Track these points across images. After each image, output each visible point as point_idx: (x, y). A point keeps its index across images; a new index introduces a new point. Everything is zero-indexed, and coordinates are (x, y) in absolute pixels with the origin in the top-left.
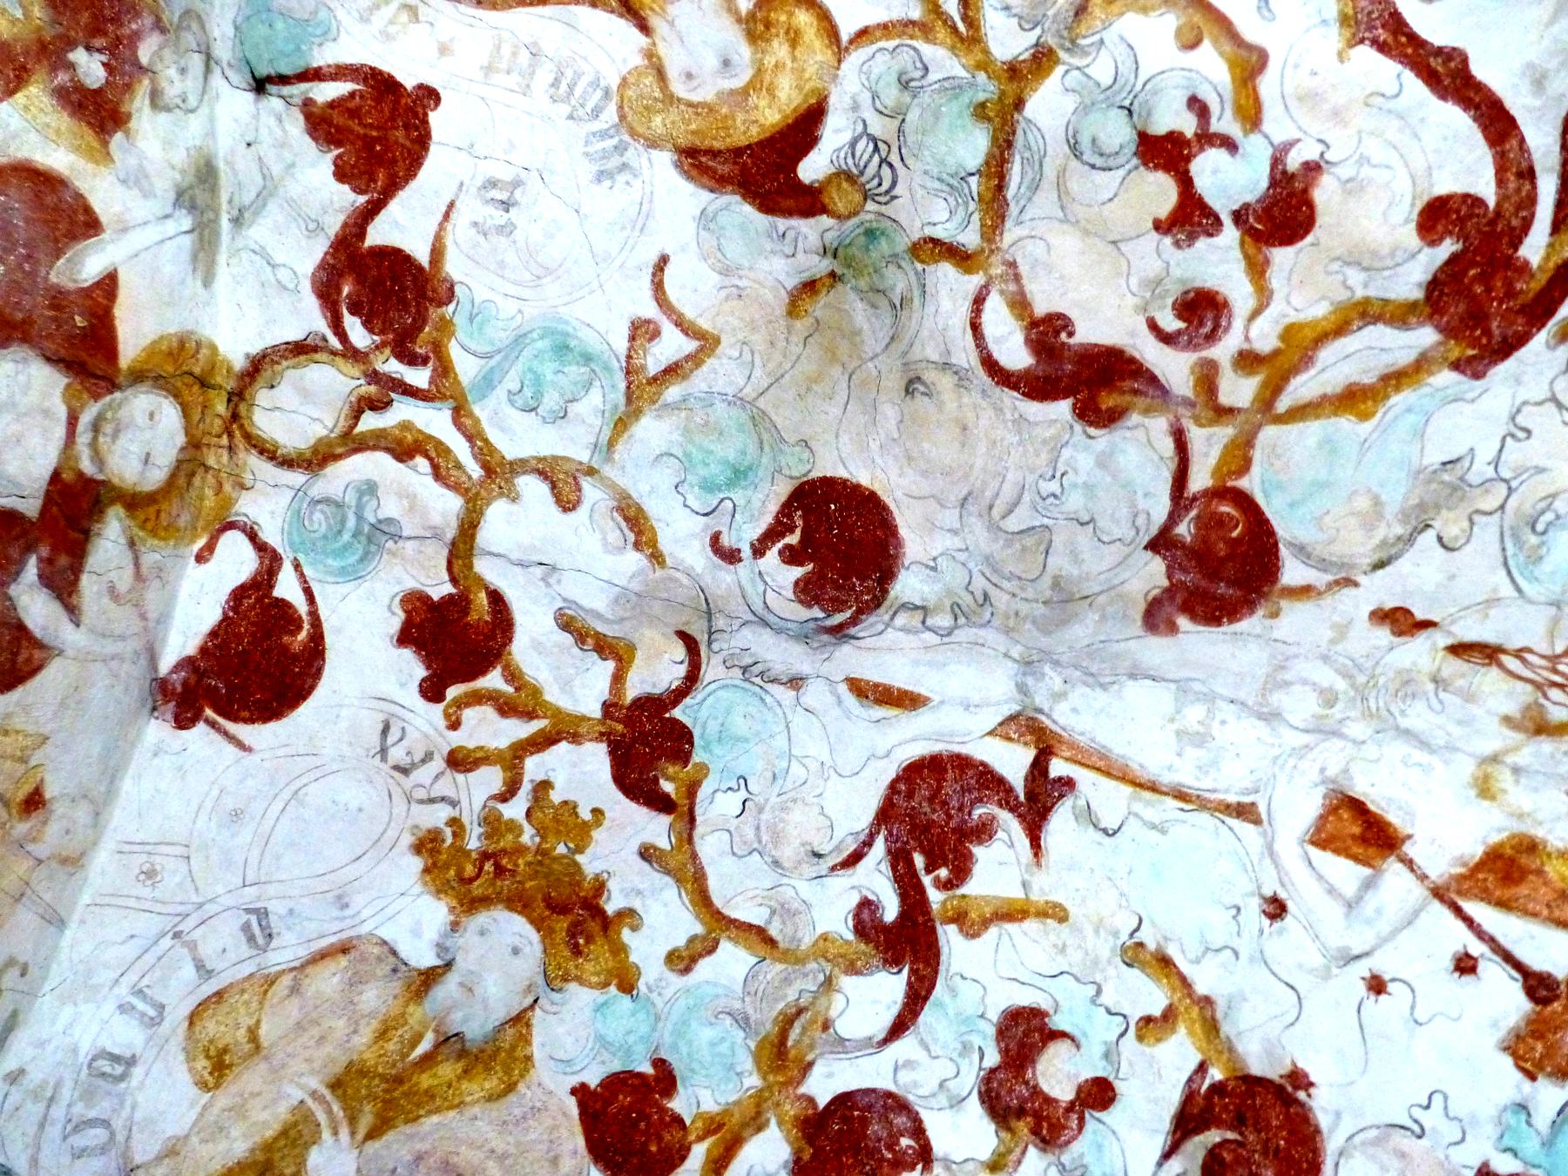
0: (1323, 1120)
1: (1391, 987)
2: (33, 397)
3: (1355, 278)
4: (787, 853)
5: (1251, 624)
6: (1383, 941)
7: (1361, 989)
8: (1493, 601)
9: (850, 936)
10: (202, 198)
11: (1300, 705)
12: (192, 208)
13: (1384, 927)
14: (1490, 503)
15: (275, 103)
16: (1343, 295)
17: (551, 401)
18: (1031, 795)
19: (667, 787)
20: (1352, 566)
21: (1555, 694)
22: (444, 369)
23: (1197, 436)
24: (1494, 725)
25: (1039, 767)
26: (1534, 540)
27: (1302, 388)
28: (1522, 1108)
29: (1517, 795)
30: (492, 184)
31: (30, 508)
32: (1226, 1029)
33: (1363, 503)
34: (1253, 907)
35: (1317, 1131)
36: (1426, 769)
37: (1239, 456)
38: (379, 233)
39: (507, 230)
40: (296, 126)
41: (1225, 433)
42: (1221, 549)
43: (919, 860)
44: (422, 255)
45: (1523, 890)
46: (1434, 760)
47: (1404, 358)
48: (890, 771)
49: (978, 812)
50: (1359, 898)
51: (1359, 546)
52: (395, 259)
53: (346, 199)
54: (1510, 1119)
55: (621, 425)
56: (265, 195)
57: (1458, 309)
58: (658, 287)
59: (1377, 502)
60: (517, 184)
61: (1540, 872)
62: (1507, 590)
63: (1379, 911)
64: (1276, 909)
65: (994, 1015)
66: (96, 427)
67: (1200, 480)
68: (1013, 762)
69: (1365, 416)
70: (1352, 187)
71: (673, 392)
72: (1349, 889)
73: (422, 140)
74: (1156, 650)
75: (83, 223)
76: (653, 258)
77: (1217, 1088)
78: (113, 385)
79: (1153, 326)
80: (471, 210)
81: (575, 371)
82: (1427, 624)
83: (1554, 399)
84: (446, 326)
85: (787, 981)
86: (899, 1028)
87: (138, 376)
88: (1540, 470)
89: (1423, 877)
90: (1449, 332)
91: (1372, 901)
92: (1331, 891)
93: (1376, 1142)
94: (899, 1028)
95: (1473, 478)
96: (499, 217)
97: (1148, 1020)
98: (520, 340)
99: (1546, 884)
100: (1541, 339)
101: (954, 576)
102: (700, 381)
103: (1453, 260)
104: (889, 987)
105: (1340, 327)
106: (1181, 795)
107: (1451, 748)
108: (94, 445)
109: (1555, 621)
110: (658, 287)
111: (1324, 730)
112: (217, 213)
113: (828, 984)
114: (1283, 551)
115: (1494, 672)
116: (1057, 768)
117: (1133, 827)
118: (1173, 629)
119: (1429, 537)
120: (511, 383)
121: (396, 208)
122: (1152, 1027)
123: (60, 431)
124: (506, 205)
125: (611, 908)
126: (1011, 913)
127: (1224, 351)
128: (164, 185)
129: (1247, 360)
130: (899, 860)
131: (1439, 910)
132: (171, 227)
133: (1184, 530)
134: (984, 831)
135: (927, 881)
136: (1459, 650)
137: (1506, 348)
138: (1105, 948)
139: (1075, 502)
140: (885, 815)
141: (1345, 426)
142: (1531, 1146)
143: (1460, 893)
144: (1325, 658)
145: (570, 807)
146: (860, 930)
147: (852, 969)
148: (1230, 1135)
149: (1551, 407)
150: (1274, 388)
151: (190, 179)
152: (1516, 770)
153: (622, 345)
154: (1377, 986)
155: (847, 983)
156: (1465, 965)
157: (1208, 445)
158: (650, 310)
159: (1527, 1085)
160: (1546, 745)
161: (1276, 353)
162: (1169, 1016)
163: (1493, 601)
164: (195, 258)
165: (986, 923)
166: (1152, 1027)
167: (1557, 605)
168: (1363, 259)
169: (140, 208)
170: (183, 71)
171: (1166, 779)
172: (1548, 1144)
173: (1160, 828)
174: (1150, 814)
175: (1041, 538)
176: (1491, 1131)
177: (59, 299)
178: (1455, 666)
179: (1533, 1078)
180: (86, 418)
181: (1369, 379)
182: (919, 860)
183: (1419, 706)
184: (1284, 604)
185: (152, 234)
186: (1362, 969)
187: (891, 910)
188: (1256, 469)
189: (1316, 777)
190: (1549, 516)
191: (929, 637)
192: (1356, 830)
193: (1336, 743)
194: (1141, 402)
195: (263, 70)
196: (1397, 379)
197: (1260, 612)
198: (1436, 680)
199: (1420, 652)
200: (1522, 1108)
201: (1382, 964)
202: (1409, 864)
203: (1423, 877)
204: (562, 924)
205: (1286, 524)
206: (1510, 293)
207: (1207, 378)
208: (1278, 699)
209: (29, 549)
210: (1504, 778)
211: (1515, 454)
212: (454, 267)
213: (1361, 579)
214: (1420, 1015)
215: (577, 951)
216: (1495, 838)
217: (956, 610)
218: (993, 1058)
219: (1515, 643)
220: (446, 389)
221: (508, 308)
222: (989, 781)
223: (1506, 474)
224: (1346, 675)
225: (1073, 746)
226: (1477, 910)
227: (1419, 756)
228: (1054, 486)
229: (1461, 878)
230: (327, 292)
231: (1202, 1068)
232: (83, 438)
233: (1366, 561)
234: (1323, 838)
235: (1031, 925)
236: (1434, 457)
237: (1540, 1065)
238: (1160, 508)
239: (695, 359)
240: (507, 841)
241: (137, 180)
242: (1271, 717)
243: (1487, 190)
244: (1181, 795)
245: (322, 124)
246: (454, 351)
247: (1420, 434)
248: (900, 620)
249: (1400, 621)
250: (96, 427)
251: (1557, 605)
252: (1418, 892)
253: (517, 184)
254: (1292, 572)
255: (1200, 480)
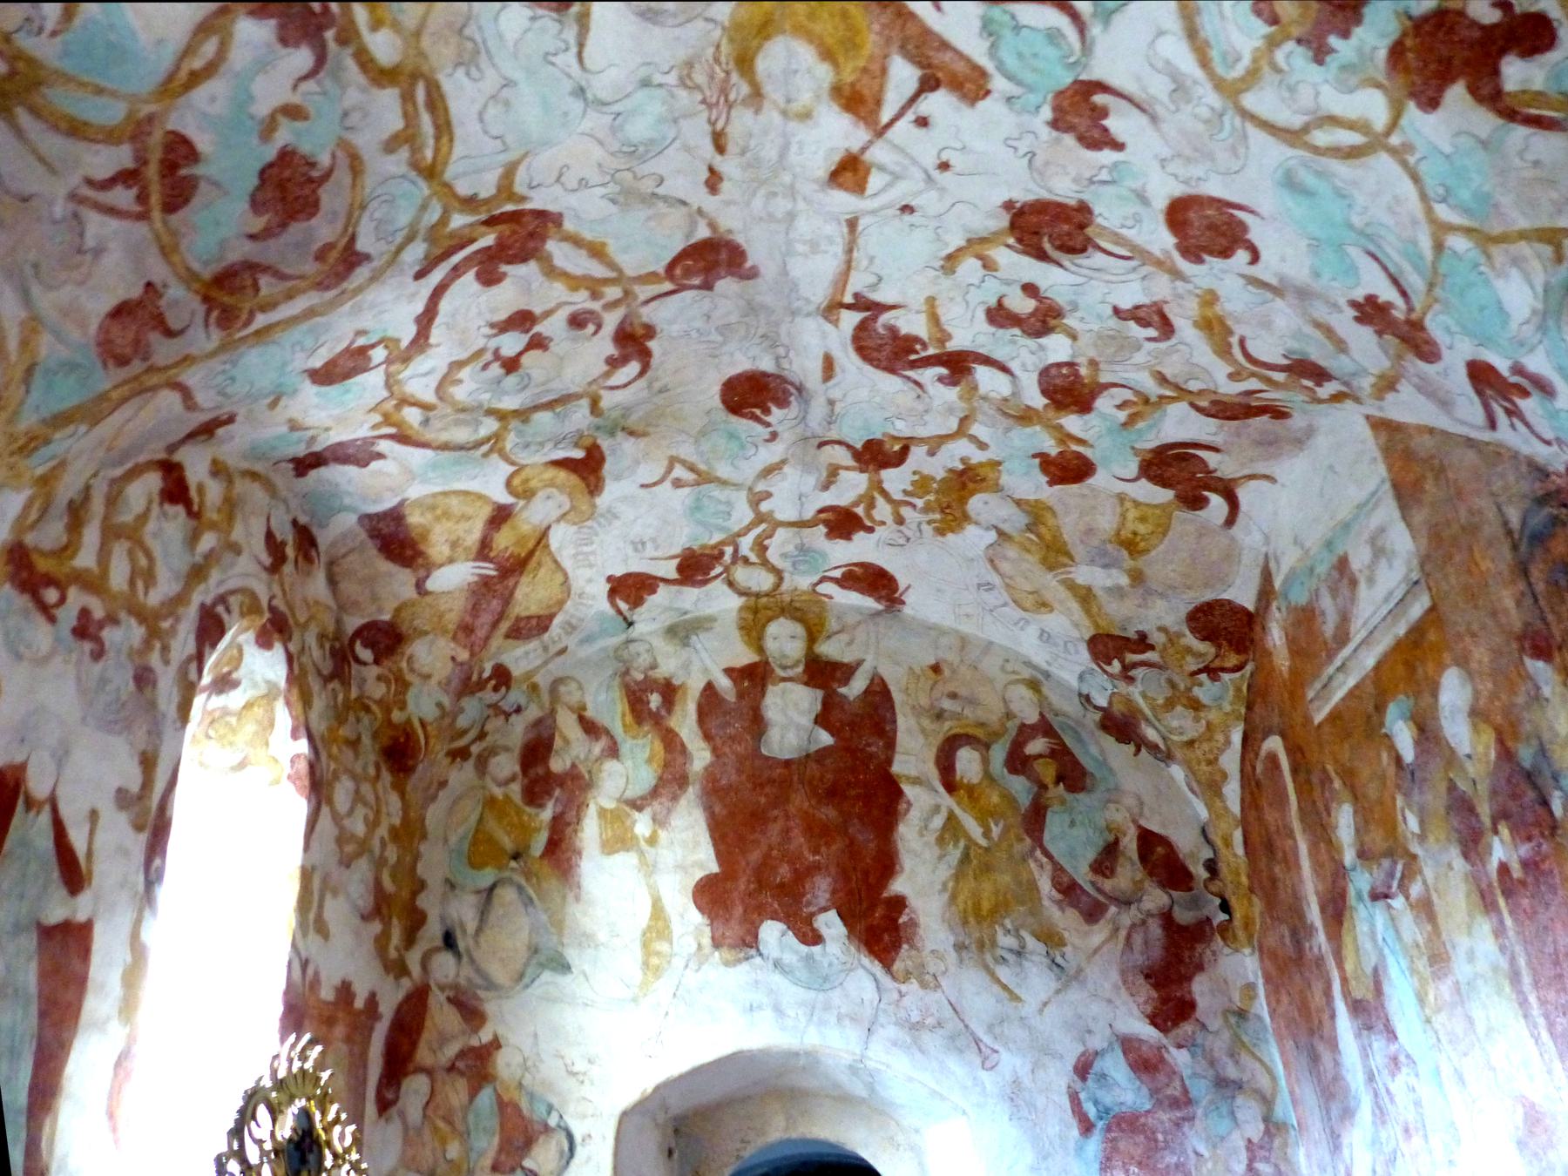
0: (1030, 197)
1: (944, 157)
2: (778, 701)
3: (535, 286)
4: (921, 408)
5: (740, 239)
6: (914, 162)
7: (947, 174)
8: (687, 149)
9: (958, 389)
10: (682, 634)
11: (781, 205)
12: (687, 637)
13: (906, 162)
14: (628, 175)
15: (635, 618)
16: (547, 284)
17: (722, 508)
18: (867, 309)
19: (897, 448)
20: (690, 216)
21: (732, 97)
22: (723, 543)
23: (642, 297)
24: (762, 118)
25: (849, 307)
26: (641, 149)
27: (598, 270)
28: (1009, 100)
29: (805, 98)
30: (636, 550)
31: (819, 694)
32: (985, 235)
33: (652, 224)
34: (907, 218)
35: (1037, 201)
36: (801, 144)
37: (651, 277)
38: (674, 575)
39: (653, 540)
40: (639, 610)
41: (637, 288)
42: (701, 264)
43: (913, 357)
44: (677, 561)
45: (866, 92)
46: (794, 140)
47: (566, 247)
48: (868, 369)
49: (881, 331)
50: (892, 173)
51: (677, 215)
52: (680, 569)
53: (663, 590)
54: (1017, 107)
55: (724, 483)
56: (670, 609)
57: (531, 245)
58: (655, 484)
59: (649, 218)
60: (633, 543)
61: (853, 85)
62: (677, 144)
63: (897, 163)
64: (907, 209)
65: (993, 329)
66: (784, 668)
67: (668, 286)
68: (850, 319)
69: (604, 245)
70: (493, 311)
71: (702, 467)
72: (887, 178)
73: (629, 575)
74: (769, 270)
75: (709, 688)
76: (643, 492)
77: (1020, 240)
78: (767, 663)
79: (596, 333)
80: (650, 551)
81: (706, 501)
82: (711, 170)
83: (558, 180)
84: (703, 547)
85: (985, 414)
86: (1004, 369)
87: (761, 650)
88: (600, 165)
89: (871, 142)
90: (543, 239)
91: (892, 167)
92: (889, 185)
93: (1041, 174)
94: (1004, 369)
95: (617, 188)
96: (649, 545)
97: (985, 267)
98: (700, 523)
99: (859, 80)
100: (528, 206)
101: (755, 351)
102: (693, 458)
103: (509, 263)
104: (982, 374)
105: (564, 275)
106: (850, 251)
107: (784, 135)
108: (792, 667)
109: (685, 116)
110: (655, 484)
111: (792, 192)
112: (686, 621)
113: (985, 398)
114: (693, 241)
115: (729, 130)
116: (848, 299)
117: (874, 269)
118: (753, 267)
119: (661, 191)
120: (720, 521)
121: (661, 574)
122: (988, 265)
123: (789, 685)
124: (643, 543)
125: (961, 467)
126: (934, 319)
127: (596, 306)
128: (685, 653)
129: (595, 295)
130: (914, 365)
131: (890, 134)
132: (699, 646)
133: (696, 281)
134: (893, 330)
135: (923, 354)
136: (720, 148)
137: (541, 215)
138: (946, 282)
139: (699, 324)
140: (891, 370)
141: (612, 249)
142: (1033, 99)
143: (876, 122)
144: (748, 204)
145: (914, 483)
146: (954, 384)
147: (975, 388)
148: (1046, 239)
149: (563, 179)
150: (606, 282)
151: (677, 641)
152: (789, 101)
153: (686, 490)
154: (944, 166)
155: (982, 390)
156: (922, 122)
157: (644, 292)
158: (667, 484)
159: (994, 95)
160: (768, 89)
161: (587, 288)
162: (980, 257)
163: (687, 149)
164: (708, 630)
165: (943, 331)
166: (988, 265)
167: (675, 121)
168: (527, 289)
169: (696, 667)
170: (639, 654)
171: (841, 256)
172: (1031, 89)
173: (872, 259)
174: (865, 263)
175: (725, 329)
176: (1026, 118)
177: (741, 695)
178: (732, 148)
179: (988, 92)
180: (782, 673)
181: (584, 252)
182: (913, 357)
183: (762, 154)
184: (722, 230)
185: (704, 655)
186: (936, 174)
187: (943, 371)
188: (652, 269)
189: (821, 195)
190: (625, 149)
191: (792, 354)
192: (849, 175)
193: (798, 185)
194: (636, 322)
195: (625, 625)
196: (576, 241)
197: (731, 237)
198: (743, 153)
199: (727, 166)
200: (1009, 100)
201: (930, 161)
202: (864, 149)
203: (871, 142)
204: (971, 486)
205: (678, 246)
206: (514, 232)
207: (614, 304)
208: (779, 215)
209: (835, 691)
210: (796, 107)
211: (595, 178)
212: (677, 550)
213: (695, 207)
214: (959, 145)
215: (983, 480)
216: (836, 108)
217: (774, 346)
218: (1016, 331)
219: (708, 128)
220: (733, 540)
221: (686, 531)
222: (862, 328)
223: (608, 178)
224: (754, 194)
225: (834, 294)
226: (885, 117)
227: (794, 148)
228: (694, 334)
229: (867, 123)
230: (705, 582)
231: (1008, 246)
232: (790, 673)
233: (684, 209)
234: (859, 188)
235: (940, 311)
236: (613, 209)
237: (980, 87)
238: (688, 295)
239: (683, 463)
240: (934, 505)
241: (686, 666)
242: (791, 216)
243: (469, 277)
244: (850, 251)
245: (637, 602)
246: (713, 542)
247: (603, 221)
248: (786, 366)
249: (714, 181)
250: (784, 668)
251: (675, 121)
252: (879, 144)
253: (633, 543)
254: (703, 233)
255: (668, 286)
